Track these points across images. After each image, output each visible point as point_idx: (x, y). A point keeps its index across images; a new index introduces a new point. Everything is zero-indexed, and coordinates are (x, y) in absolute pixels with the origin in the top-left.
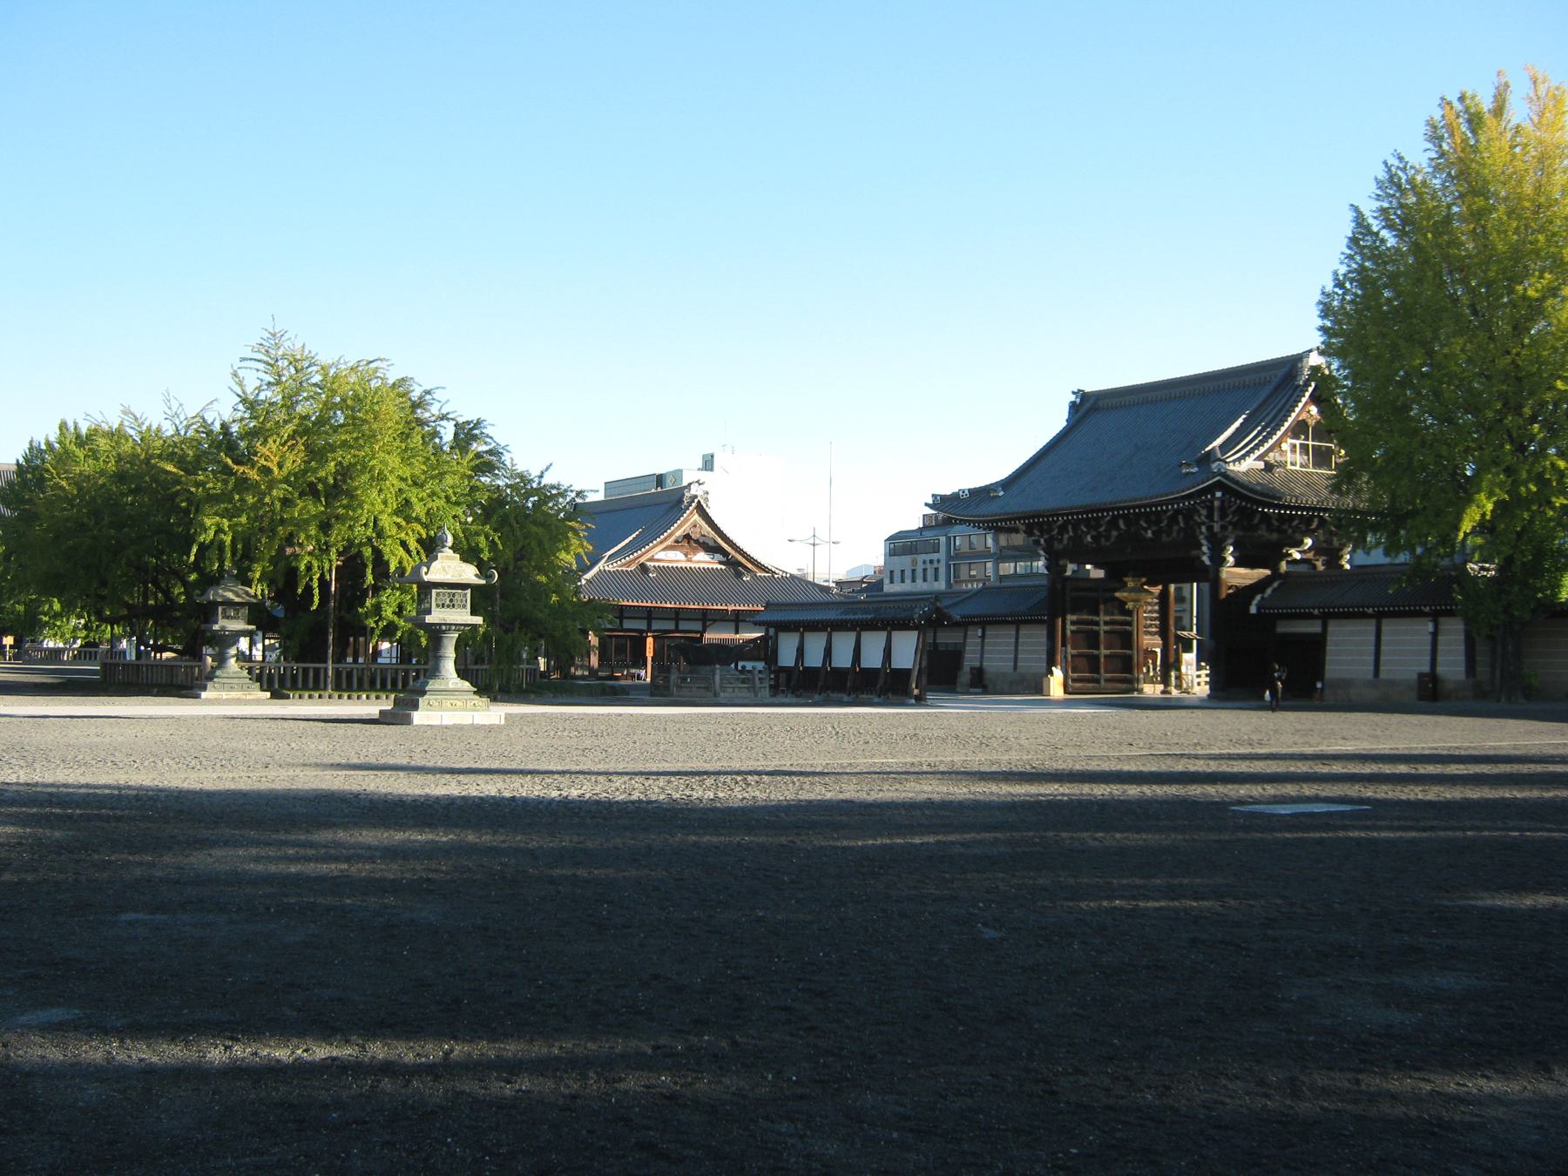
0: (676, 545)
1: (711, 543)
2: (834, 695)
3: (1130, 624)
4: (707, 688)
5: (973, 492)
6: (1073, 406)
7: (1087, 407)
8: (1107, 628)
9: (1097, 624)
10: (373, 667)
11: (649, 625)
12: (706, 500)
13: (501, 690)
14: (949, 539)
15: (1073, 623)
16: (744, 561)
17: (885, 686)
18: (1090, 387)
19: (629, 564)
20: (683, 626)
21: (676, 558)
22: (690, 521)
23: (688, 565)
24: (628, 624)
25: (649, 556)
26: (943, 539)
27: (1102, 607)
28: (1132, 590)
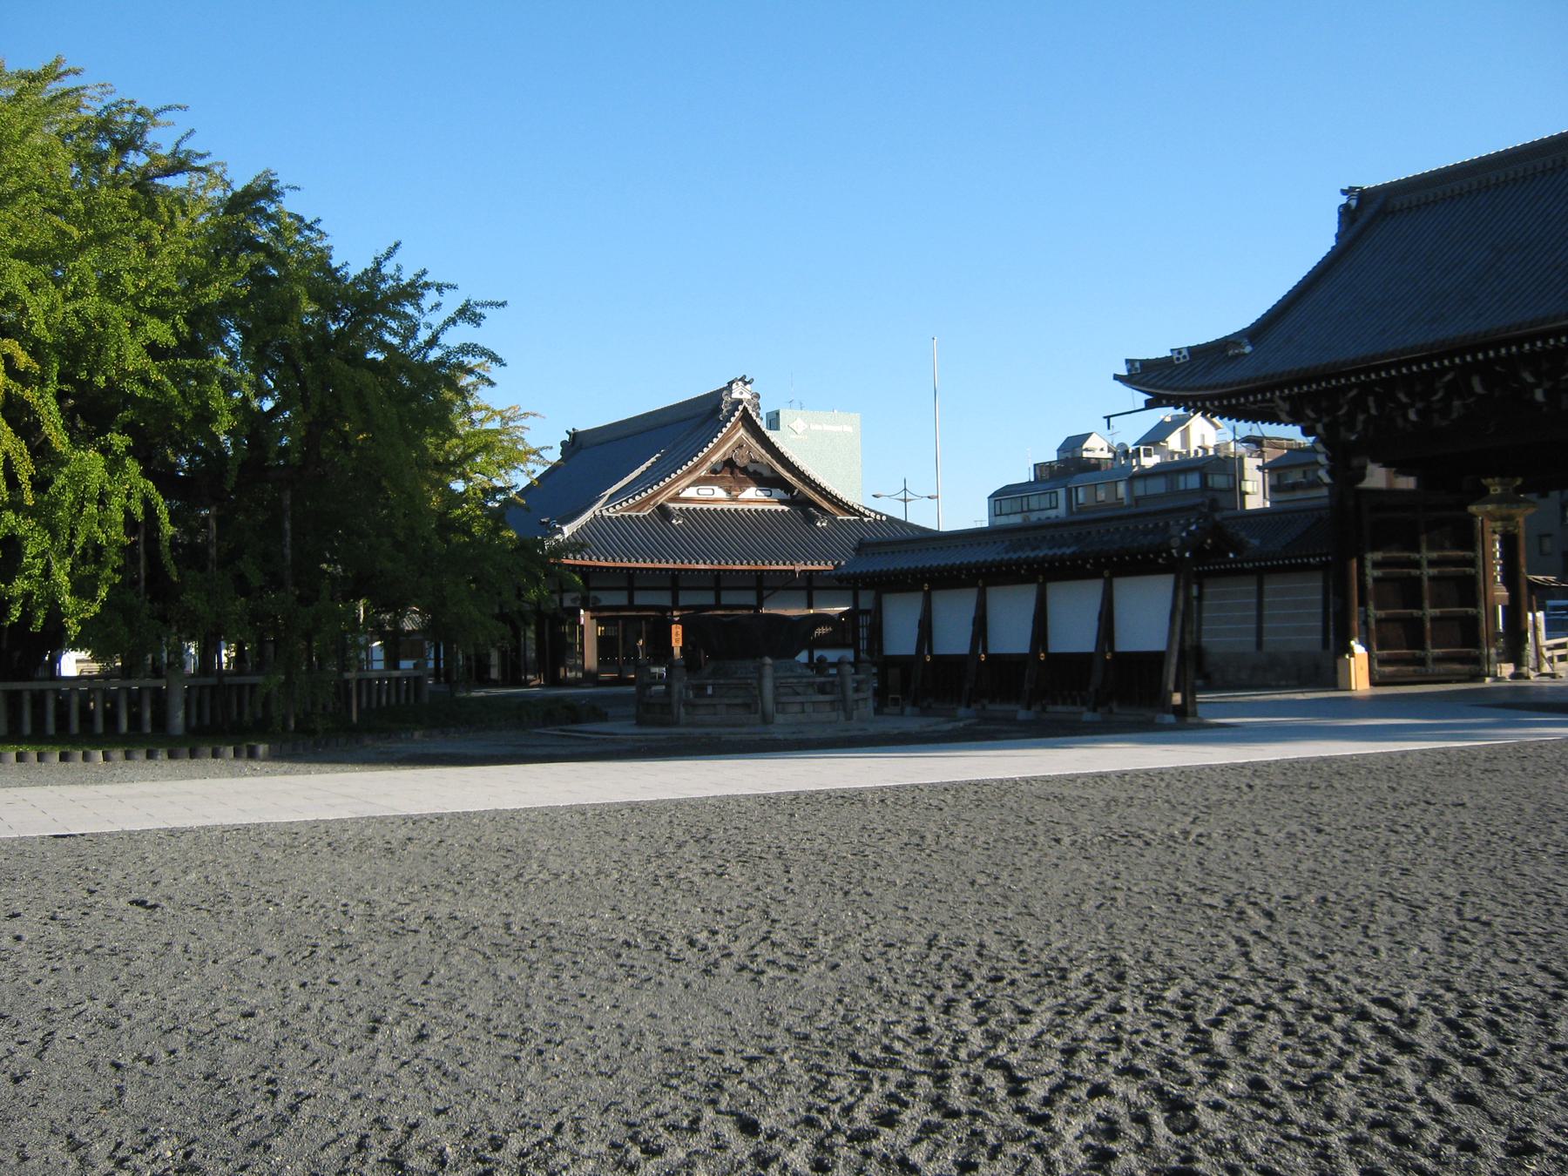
0: (712, 478)
1: (766, 473)
2: (997, 708)
3: (1471, 563)
4: (747, 706)
5: (1197, 352)
6: (1346, 213)
7: (1367, 213)
8: (1433, 571)
9: (1416, 564)
10: (396, 673)
11: (675, 599)
12: (757, 407)
13: (305, 729)
14: (1069, 492)
15: (1376, 565)
16: (816, 498)
17: (1120, 693)
18: (1369, 181)
19: (640, 506)
20: (728, 598)
21: (715, 495)
22: (731, 441)
23: (733, 506)
24: (641, 599)
25: (671, 492)
26: (1062, 492)
27: (1423, 538)
28: (1499, 500)
